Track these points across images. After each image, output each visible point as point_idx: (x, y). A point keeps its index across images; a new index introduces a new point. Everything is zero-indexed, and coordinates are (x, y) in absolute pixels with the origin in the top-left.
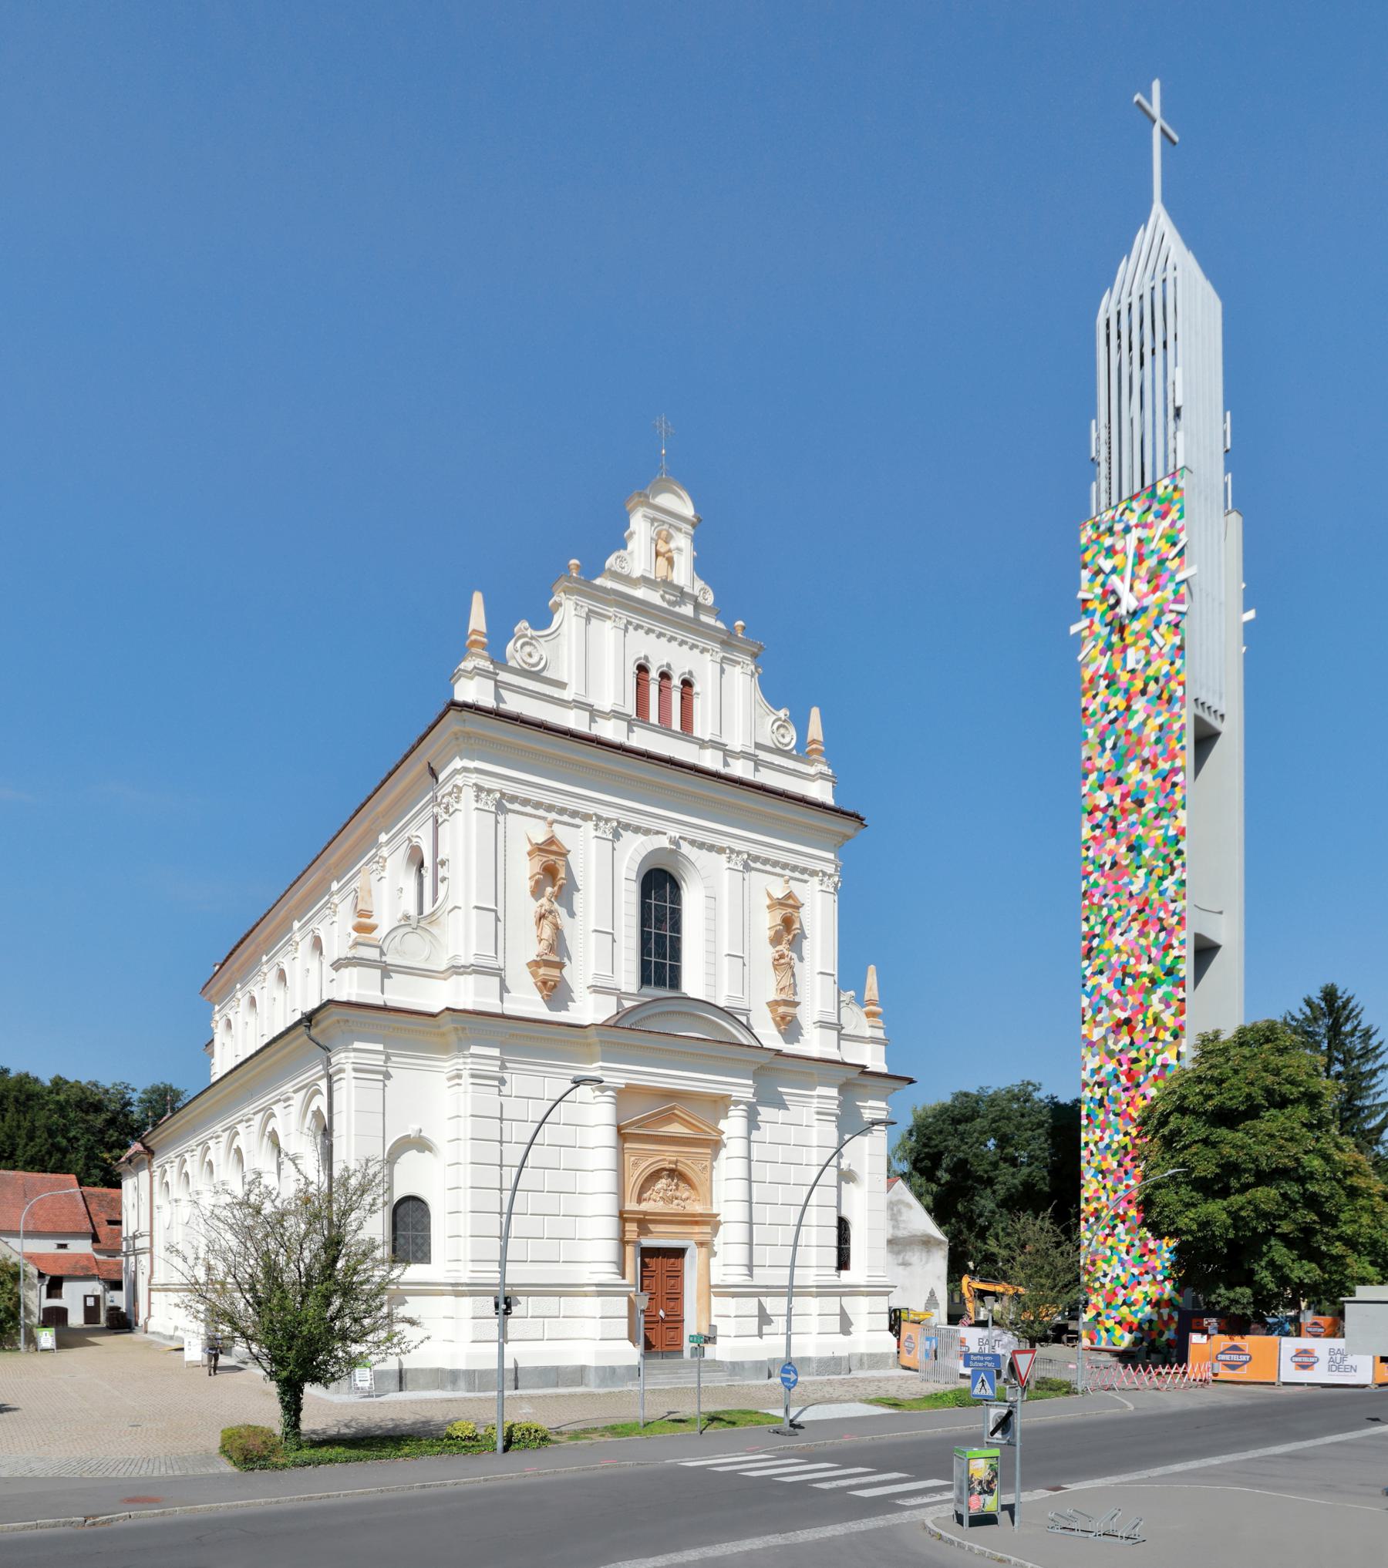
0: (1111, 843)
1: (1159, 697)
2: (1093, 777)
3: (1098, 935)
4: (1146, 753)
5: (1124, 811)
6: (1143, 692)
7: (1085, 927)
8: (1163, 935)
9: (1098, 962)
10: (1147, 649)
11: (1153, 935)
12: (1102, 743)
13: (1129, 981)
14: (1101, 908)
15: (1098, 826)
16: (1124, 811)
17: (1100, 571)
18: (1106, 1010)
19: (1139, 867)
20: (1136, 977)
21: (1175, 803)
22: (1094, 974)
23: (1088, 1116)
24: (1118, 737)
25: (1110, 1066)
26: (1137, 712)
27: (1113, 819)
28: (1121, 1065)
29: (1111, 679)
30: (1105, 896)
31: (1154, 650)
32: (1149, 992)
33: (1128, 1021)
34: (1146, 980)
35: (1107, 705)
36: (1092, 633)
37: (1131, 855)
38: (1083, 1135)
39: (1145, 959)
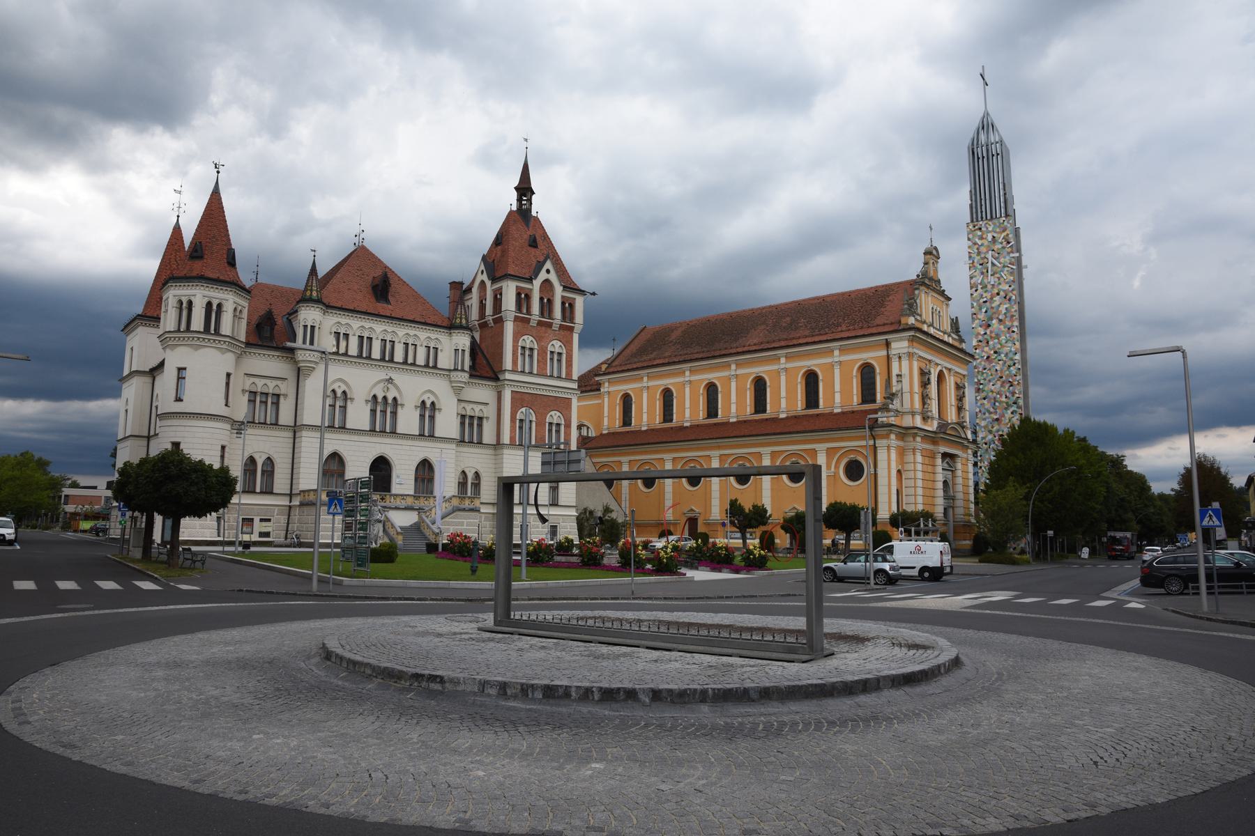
0: (986, 349)
1: (1005, 298)
2: (977, 321)
3: (982, 384)
4: (1000, 317)
5: (991, 337)
6: (998, 294)
7: (976, 380)
8: (1011, 388)
9: (984, 395)
10: (999, 278)
11: (1007, 388)
12: (980, 309)
13: (997, 404)
14: (983, 373)
15: (980, 341)
16: (991, 337)
17: (975, 244)
18: (987, 415)
19: (999, 360)
20: (1001, 402)
21: (1014, 338)
22: (980, 399)
23: (981, 456)
24: (987, 308)
25: (990, 437)
26: (995, 301)
27: (986, 339)
28: (995, 437)
29: (984, 287)
30: (985, 369)
31: (1002, 279)
32: (1006, 409)
33: (997, 420)
34: (1005, 404)
35: (982, 295)
36: (974, 266)
37: (996, 355)
38: (979, 463)
39: (1004, 396)
